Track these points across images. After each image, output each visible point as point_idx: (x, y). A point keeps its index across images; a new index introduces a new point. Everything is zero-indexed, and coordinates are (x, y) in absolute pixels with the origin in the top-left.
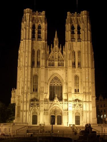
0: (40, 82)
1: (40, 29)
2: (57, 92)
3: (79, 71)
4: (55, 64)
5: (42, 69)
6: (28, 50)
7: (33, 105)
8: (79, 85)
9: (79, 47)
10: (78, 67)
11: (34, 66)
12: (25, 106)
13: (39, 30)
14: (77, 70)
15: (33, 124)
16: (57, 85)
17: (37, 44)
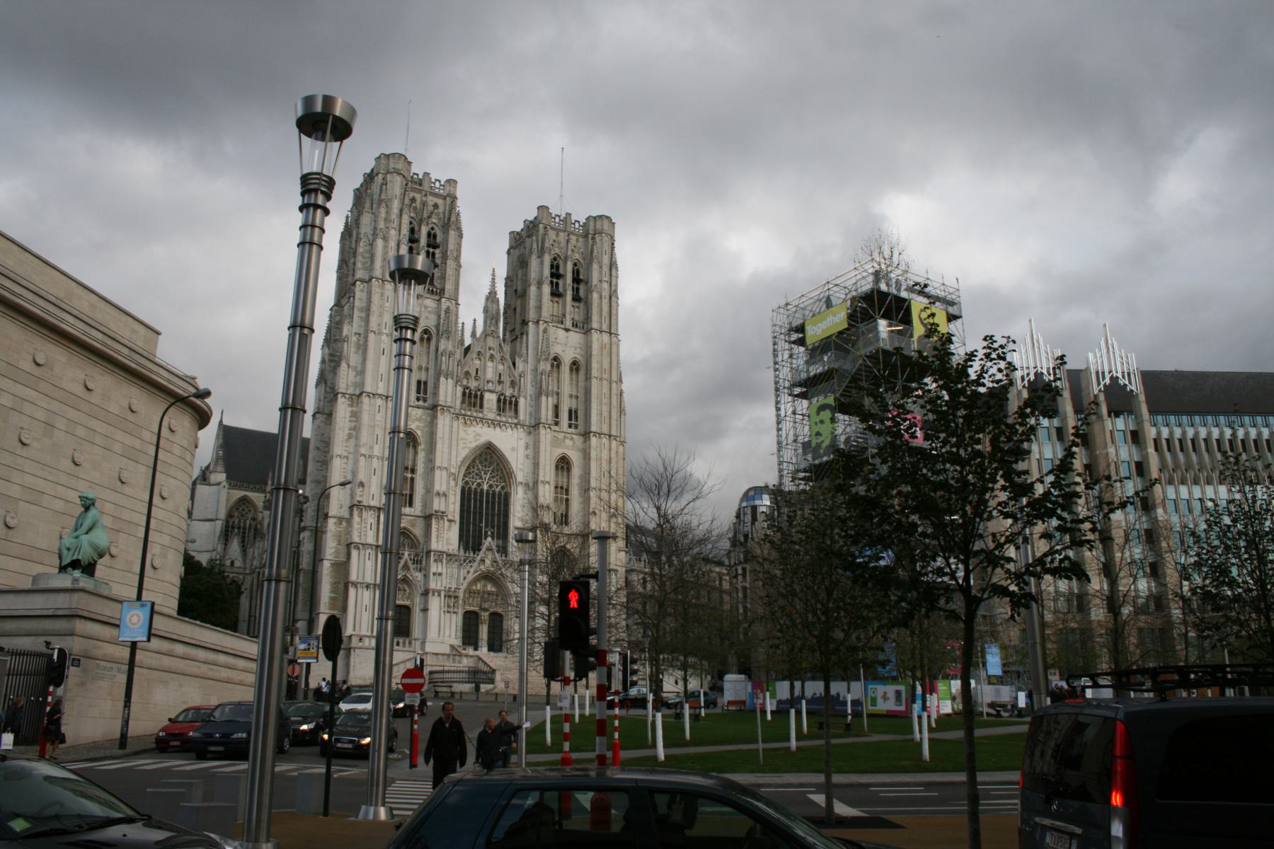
1: (435, 246)
2: (487, 514)
9: (575, 349)
10: (570, 426)
14: (565, 437)
16: (491, 486)
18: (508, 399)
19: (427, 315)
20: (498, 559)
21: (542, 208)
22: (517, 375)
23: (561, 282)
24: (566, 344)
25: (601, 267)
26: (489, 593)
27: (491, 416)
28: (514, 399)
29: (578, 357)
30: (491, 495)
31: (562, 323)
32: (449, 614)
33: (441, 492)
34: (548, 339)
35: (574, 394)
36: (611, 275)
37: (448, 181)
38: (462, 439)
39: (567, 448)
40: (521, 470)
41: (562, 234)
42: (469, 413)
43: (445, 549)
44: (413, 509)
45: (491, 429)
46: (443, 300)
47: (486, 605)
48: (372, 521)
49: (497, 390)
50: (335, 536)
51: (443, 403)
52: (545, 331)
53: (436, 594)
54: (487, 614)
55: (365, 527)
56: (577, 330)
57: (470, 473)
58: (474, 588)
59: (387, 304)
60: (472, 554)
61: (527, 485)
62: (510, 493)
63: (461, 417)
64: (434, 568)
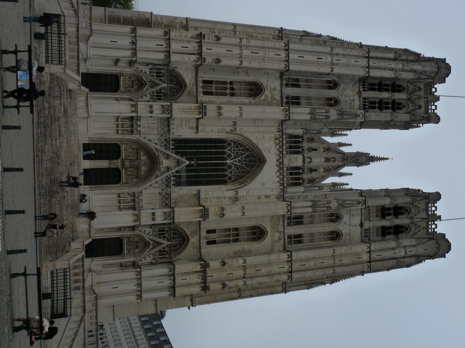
0: (240, 103)
2: (206, 165)
3: (276, 239)
4: (295, 156)
5: (283, 110)
6: (337, 64)
7: (157, 76)
8: (231, 243)
9: (349, 234)
10: (289, 237)
11: (287, 85)
12: (152, 44)
13: (390, 106)
14: (280, 232)
15: (82, 73)
16: (230, 167)
17: (354, 96)
18: (301, 176)
19: (349, 101)
20: (171, 172)
21: (437, 196)
22: (318, 185)
23: (392, 217)
24: (350, 225)
25: (414, 246)
26: (138, 169)
27: (286, 162)
28: (301, 181)
29: (344, 237)
30: (222, 167)
31: (365, 220)
32: (115, 126)
33: (222, 111)
34: (353, 205)
35: (315, 237)
36: (411, 257)
37: (438, 116)
38: (264, 137)
39: (273, 236)
40: (248, 193)
41: (425, 212)
42: (284, 142)
43: (174, 116)
44: (202, 95)
45: (276, 163)
46: (363, 111)
47: (127, 164)
48: (190, 48)
49: (305, 165)
50: (172, 22)
51: (291, 111)
52: (359, 203)
53: (133, 109)
54: (120, 165)
55: (184, 42)
56: (363, 233)
57: (237, 147)
58: (142, 153)
59: (353, 61)
60: (172, 147)
61: (236, 199)
62: (227, 185)
63: (280, 134)
64: (157, 106)
